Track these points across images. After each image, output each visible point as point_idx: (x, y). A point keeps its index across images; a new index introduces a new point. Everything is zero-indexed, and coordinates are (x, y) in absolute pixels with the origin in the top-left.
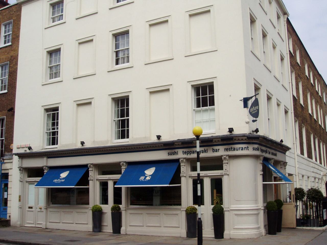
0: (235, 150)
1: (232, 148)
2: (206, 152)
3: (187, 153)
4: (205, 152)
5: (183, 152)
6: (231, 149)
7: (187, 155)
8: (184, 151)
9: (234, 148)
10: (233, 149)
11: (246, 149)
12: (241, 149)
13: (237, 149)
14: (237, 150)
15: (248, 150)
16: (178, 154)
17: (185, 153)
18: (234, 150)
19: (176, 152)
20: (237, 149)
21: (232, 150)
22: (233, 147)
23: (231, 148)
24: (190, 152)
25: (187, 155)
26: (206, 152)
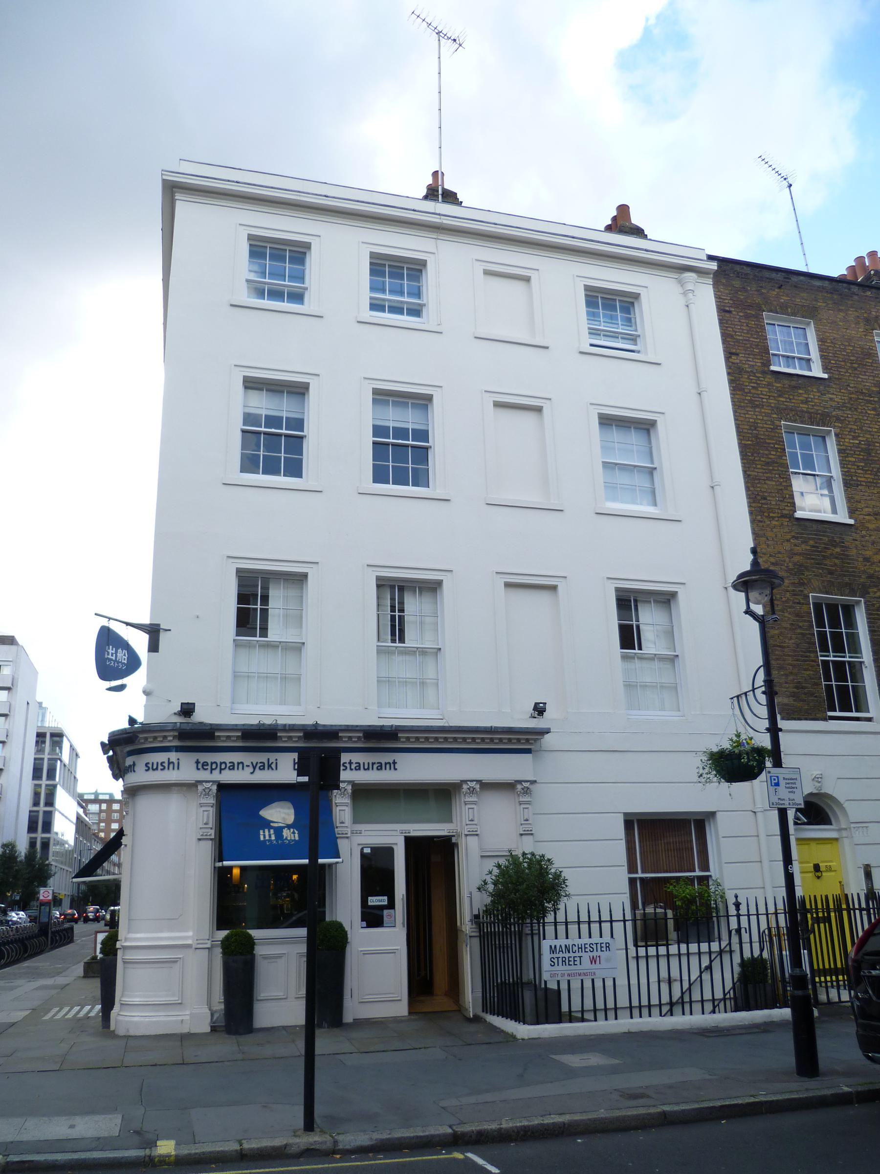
0: (359, 769)
1: (350, 763)
2: (272, 769)
3: (209, 767)
4: (268, 769)
5: (197, 762)
6: (348, 765)
7: (211, 773)
8: (202, 761)
9: (356, 763)
10: (353, 766)
11: (390, 769)
12: (375, 766)
13: (366, 767)
14: (365, 769)
15: (395, 769)
16: (178, 769)
17: (203, 765)
18: (356, 769)
19: (173, 763)
20: (366, 767)
21: (351, 769)
22: (202, 761)
23: (348, 761)
24: (221, 763)
25: (211, 773)
26: (273, 766)
